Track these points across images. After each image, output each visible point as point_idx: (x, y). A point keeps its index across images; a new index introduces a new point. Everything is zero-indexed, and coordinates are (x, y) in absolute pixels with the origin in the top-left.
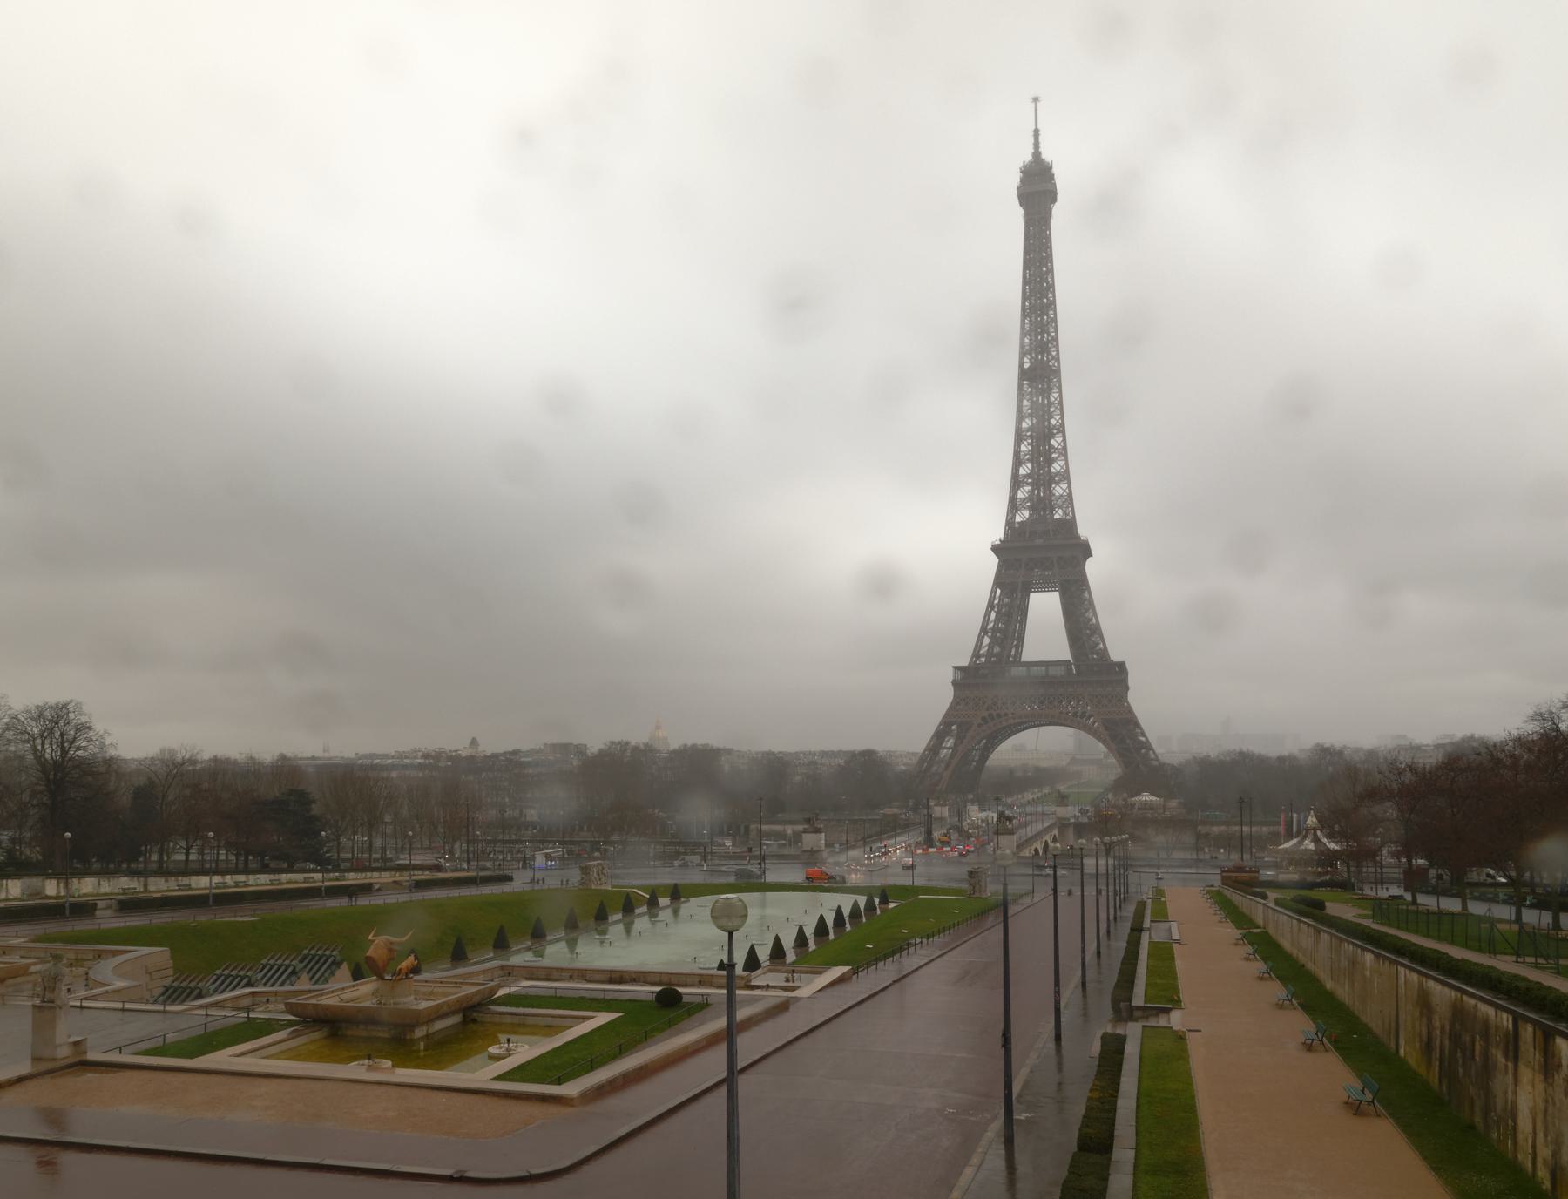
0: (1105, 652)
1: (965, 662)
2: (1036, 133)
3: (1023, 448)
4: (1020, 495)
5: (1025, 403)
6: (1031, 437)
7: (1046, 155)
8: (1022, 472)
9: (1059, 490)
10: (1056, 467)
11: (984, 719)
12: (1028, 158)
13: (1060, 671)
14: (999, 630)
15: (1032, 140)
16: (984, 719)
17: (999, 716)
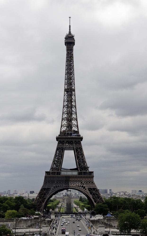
0: (87, 168)
1: (48, 170)
2: (70, 26)
3: (64, 110)
4: (63, 123)
5: (65, 98)
6: (67, 107)
7: (72, 33)
8: (64, 117)
9: (74, 122)
10: (74, 116)
11: (54, 187)
12: (68, 33)
13: (75, 173)
14: (56, 161)
15: (69, 28)
16: (54, 187)
17: (58, 186)
